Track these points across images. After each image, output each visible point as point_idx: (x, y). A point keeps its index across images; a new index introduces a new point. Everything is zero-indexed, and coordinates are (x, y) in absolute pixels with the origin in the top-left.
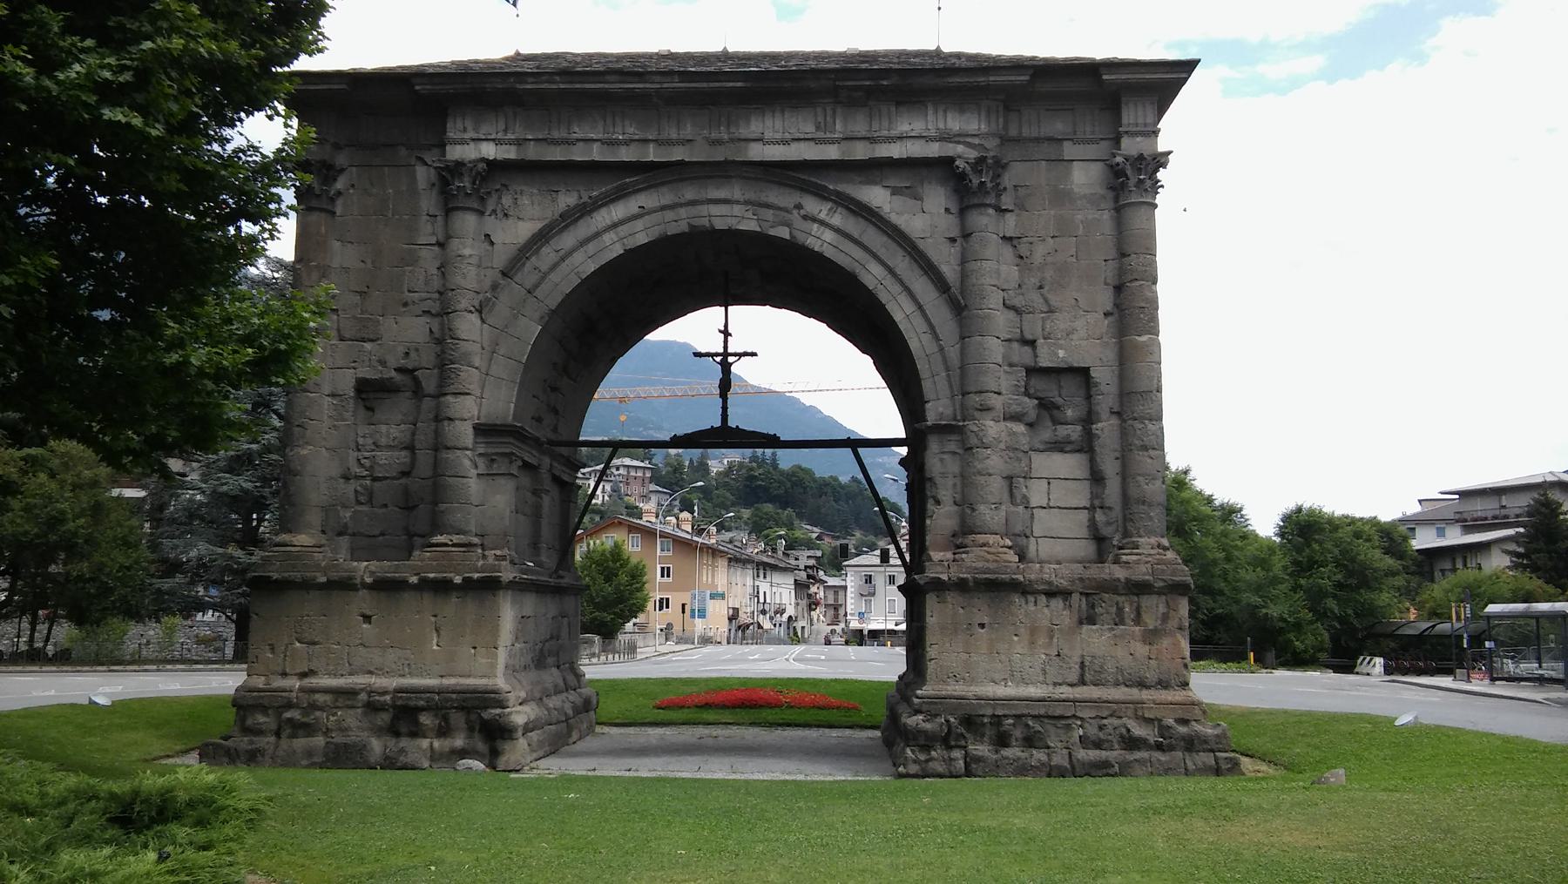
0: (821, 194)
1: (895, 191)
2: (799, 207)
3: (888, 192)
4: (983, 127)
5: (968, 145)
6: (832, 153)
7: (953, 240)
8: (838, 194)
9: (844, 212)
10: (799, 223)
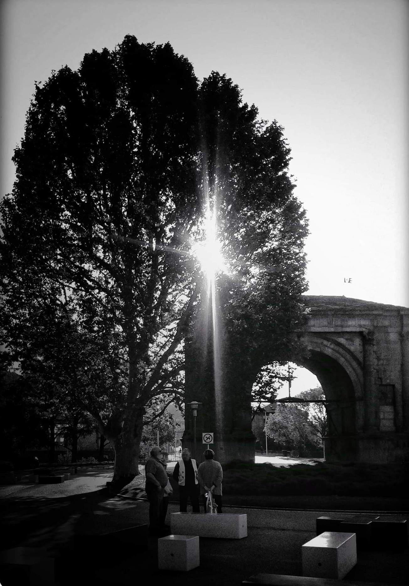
0: (328, 340)
1: (347, 339)
2: (322, 343)
3: (345, 339)
4: (370, 324)
5: (366, 329)
6: (332, 330)
7: (361, 352)
8: (333, 340)
9: (334, 345)
10: (322, 348)
